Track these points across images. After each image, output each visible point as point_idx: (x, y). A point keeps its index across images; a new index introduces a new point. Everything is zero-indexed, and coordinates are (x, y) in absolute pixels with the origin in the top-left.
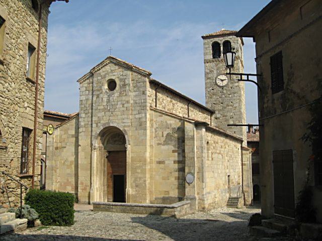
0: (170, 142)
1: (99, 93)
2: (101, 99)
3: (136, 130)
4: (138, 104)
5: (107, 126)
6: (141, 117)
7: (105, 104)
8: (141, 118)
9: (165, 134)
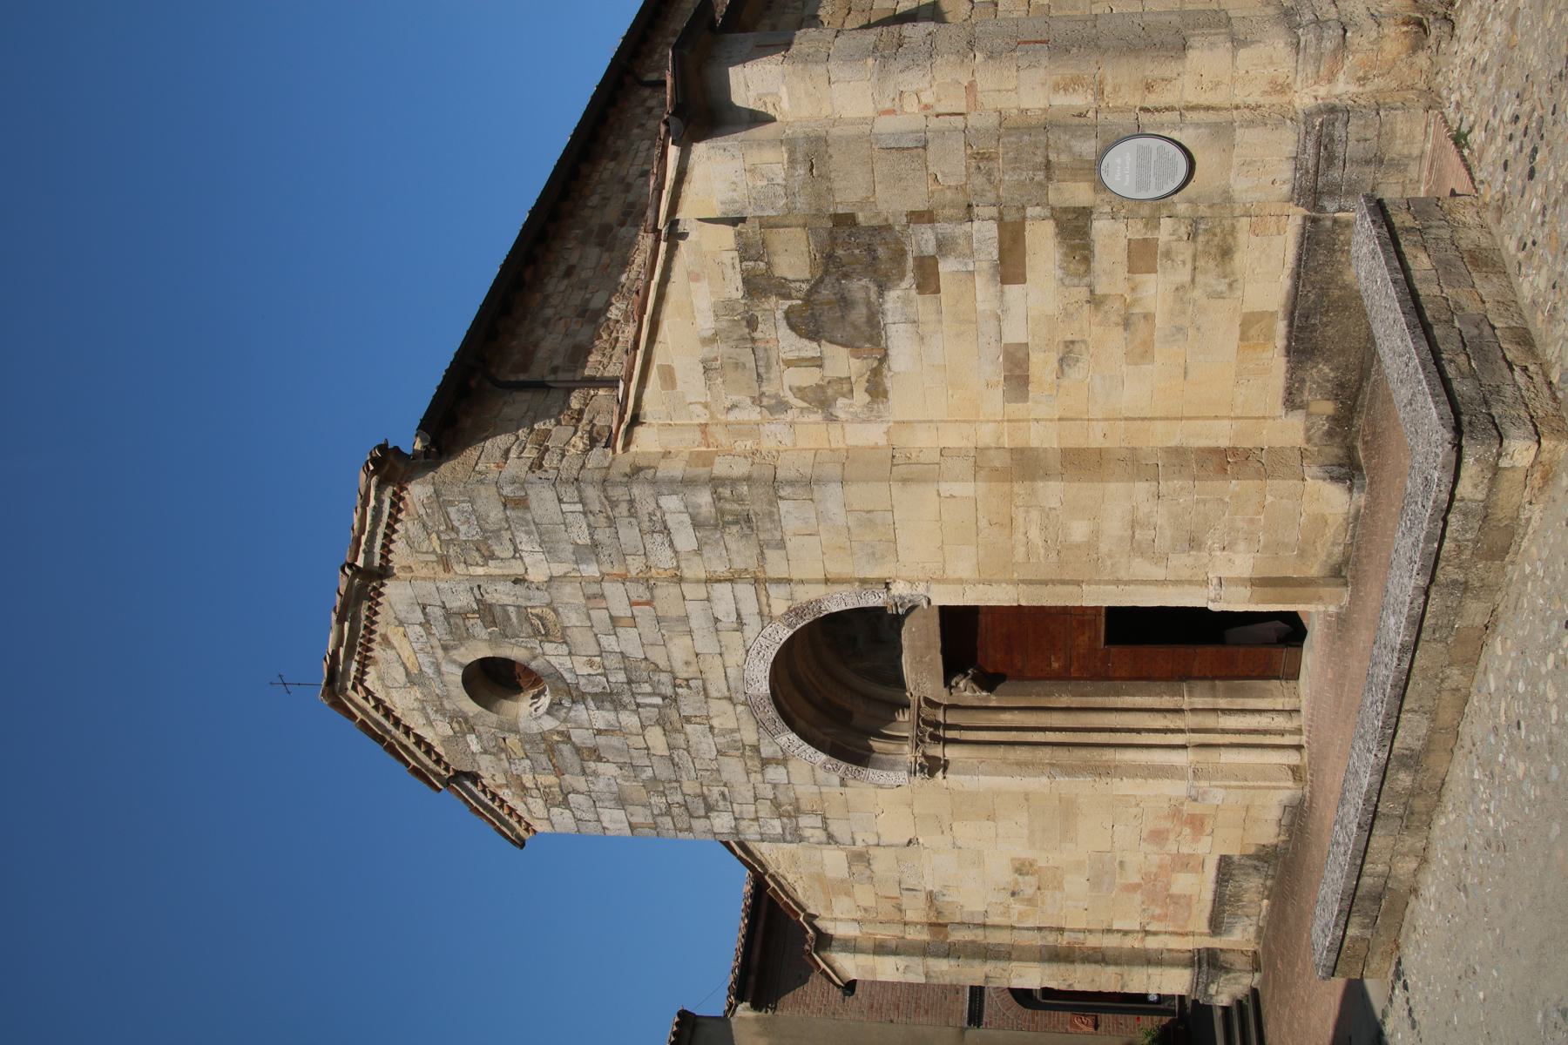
0: (859, 314)
1: (566, 749)
2: (601, 740)
3: (781, 545)
4: (603, 535)
5: (771, 712)
6: (686, 518)
7: (629, 720)
8: (692, 518)
9: (788, 343)
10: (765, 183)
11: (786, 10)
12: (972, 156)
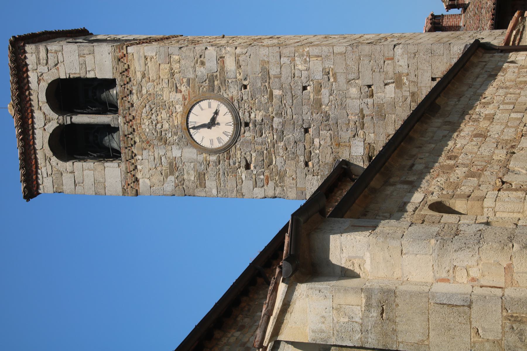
10: (347, 320)
11: (377, 217)
12: (508, 318)
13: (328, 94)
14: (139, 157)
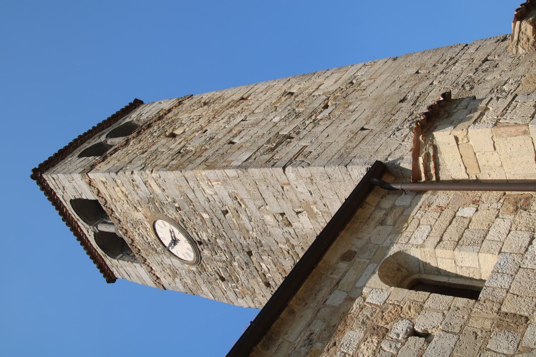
13: (247, 221)
14: (148, 261)
